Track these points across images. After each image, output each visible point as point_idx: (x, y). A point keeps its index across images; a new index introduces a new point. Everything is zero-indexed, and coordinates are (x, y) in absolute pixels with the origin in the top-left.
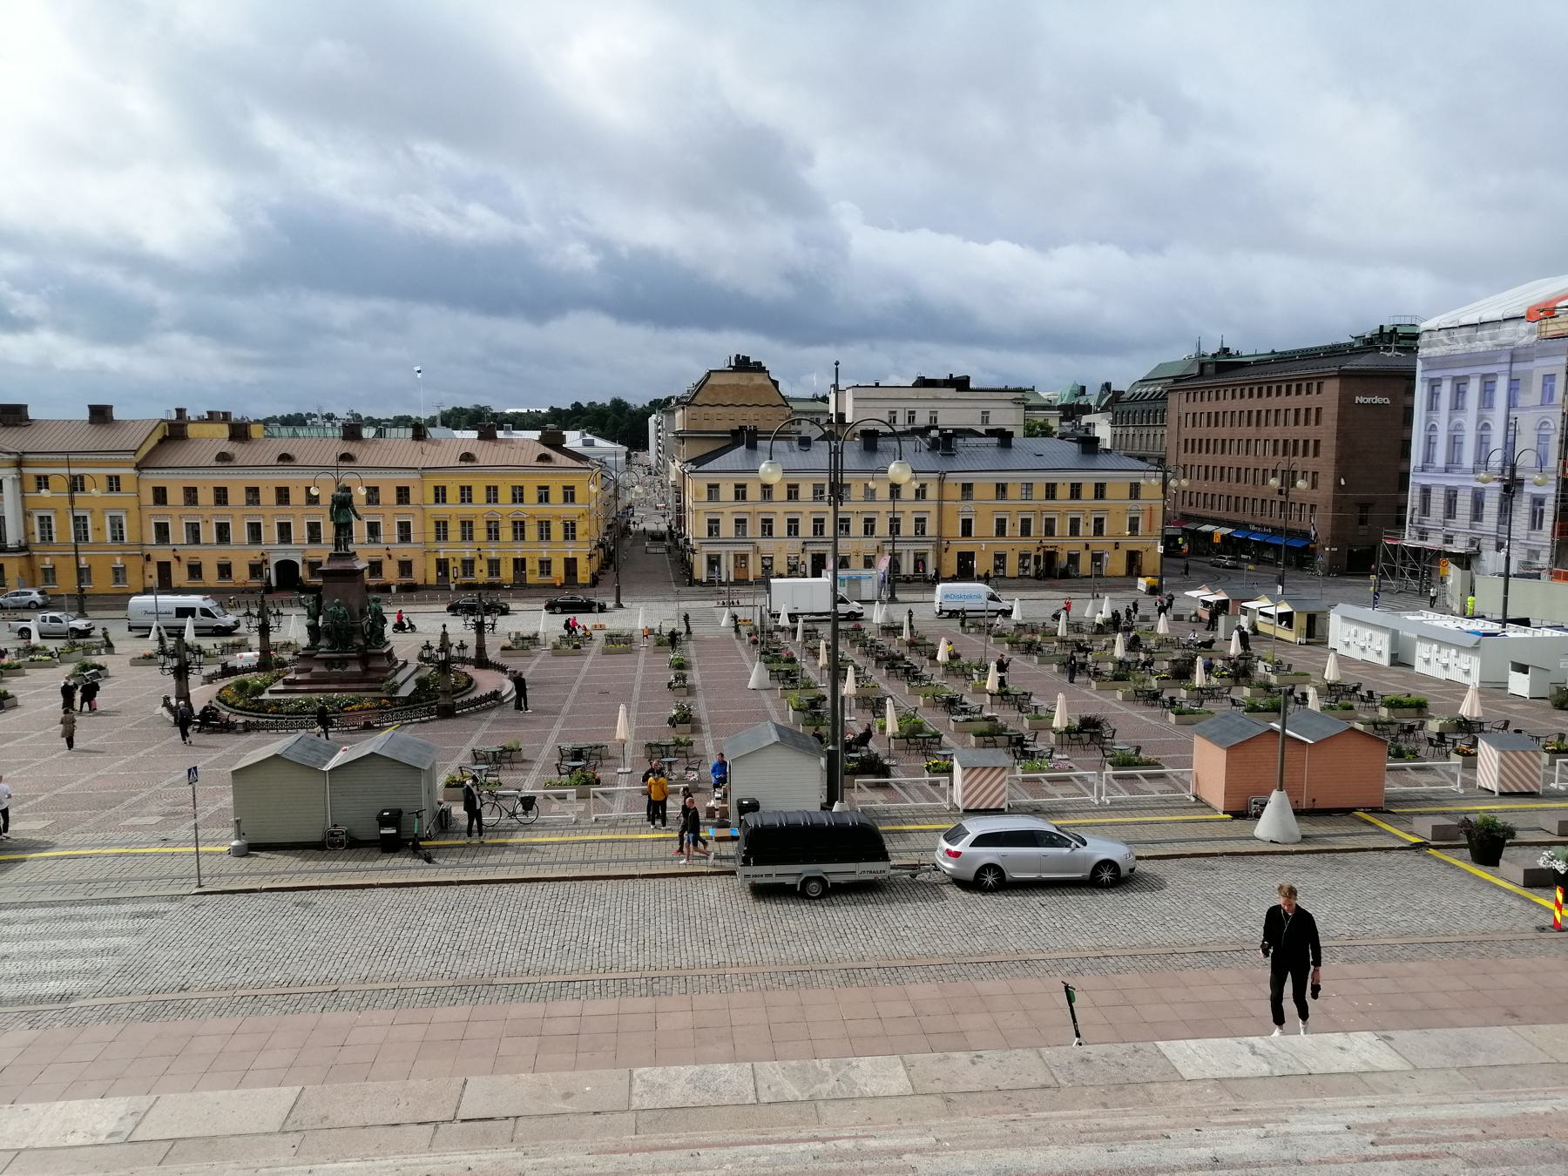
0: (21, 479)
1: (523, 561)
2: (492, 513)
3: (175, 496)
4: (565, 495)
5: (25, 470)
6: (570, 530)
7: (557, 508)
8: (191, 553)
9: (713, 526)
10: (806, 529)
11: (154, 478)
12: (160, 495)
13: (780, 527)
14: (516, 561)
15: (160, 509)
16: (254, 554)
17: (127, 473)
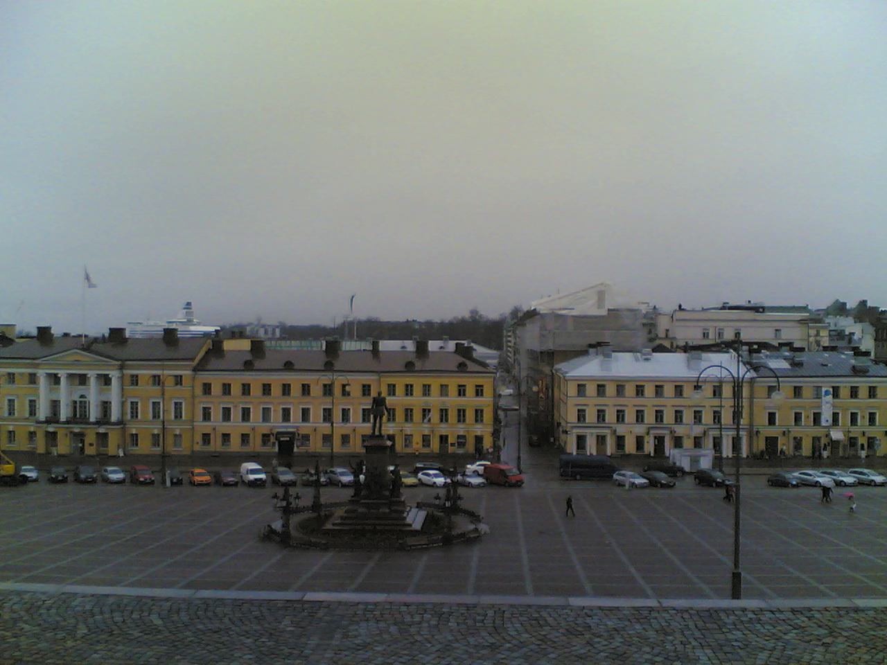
0: (122, 378)
1: (447, 437)
3: (216, 389)
5: (125, 372)
6: (479, 414)
7: (470, 401)
8: (225, 427)
9: (581, 415)
10: (649, 418)
11: (205, 377)
12: (207, 388)
13: (630, 416)
14: (441, 437)
15: (206, 399)
16: (265, 428)
17: (186, 373)
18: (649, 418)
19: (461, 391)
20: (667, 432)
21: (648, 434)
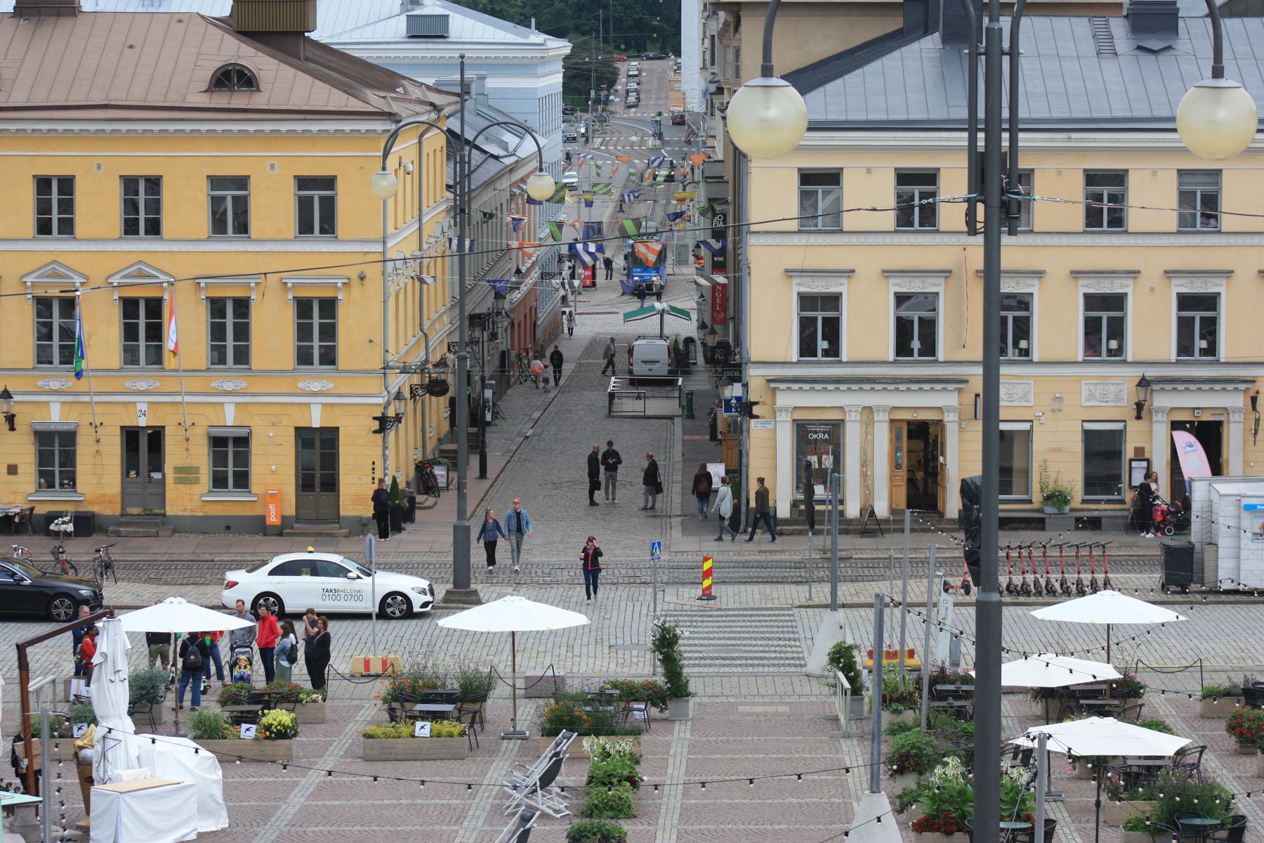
1: (156, 437)
2: (54, 270)
4: (304, 206)
6: (317, 323)
7: (274, 255)
9: (820, 326)
10: (1151, 331)
14: (131, 436)
18: (1151, 331)
19: (230, 210)
20: (1236, 401)
21: (1140, 409)
